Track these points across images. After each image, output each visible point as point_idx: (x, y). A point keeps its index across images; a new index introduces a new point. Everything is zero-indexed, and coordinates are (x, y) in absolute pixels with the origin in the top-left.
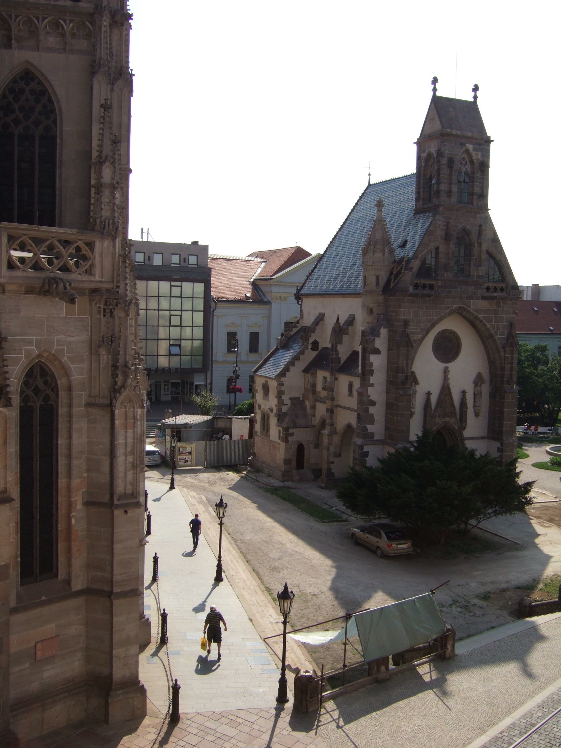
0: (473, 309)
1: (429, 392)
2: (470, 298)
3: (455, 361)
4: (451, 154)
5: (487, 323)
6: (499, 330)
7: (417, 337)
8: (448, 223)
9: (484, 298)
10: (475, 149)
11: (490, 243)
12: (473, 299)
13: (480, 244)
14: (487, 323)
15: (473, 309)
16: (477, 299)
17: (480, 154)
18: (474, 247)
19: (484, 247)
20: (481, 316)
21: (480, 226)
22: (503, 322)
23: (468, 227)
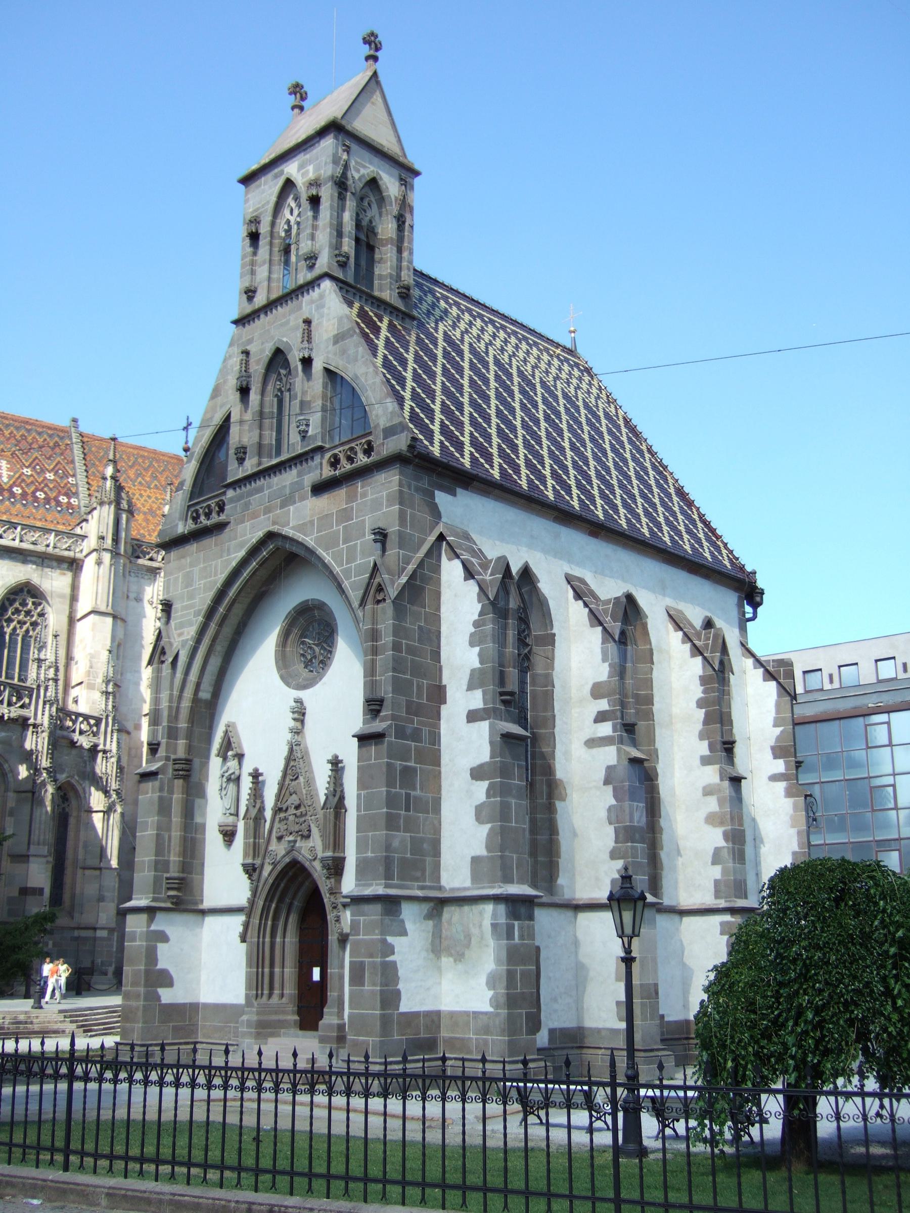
0: (292, 528)
1: (256, 770)
2: (288, 501)
3: (325, 679)
4: (258, 209)
5: (324, 554)
6: (355, 560)
7: (188, 633)
8: (247, 353)
9: (320, 489)
10: (301, 167)
11: (331, 347)
12: (294, 503)
13: (307, 362)
14: (324, 554)
15: (292, 528)
16: (302, 499)
17: (311, 168)
18: (297, 376)
19: (318, 366)
20: (309, 541)
21: (308, 322)
22: (364, 535)
23: (285, 339)
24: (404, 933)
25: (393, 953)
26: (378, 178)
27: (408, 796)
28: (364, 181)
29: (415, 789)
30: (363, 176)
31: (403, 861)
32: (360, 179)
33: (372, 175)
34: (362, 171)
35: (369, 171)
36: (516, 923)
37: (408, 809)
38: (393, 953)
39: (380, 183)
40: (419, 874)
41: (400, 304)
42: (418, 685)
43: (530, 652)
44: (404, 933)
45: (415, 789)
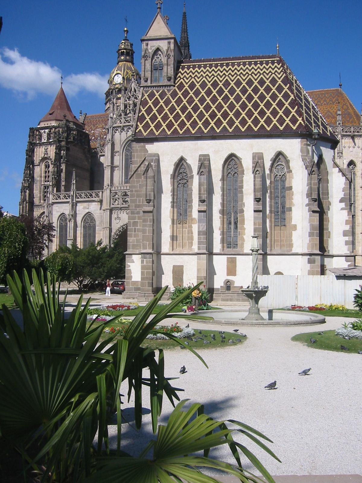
24: (133, 262)
25: (130, 267)
26: (159, 47)
27: (135, 229)
28: (153, 51)
29: (138, 227)
30: (154, 49)
31: (133, 245)
32: (152, 51)
33: (157, 47)
34: (153, 48)
35: (155, 47)
36: (145, 260)
37: (135, 232)
38: (130, 267)
39: (160, 48)
40: (139, 248)
41: (169, 83)
42: (139, 199)
43: (187, 182)
44: (133, 262)
45: (138, 227)
